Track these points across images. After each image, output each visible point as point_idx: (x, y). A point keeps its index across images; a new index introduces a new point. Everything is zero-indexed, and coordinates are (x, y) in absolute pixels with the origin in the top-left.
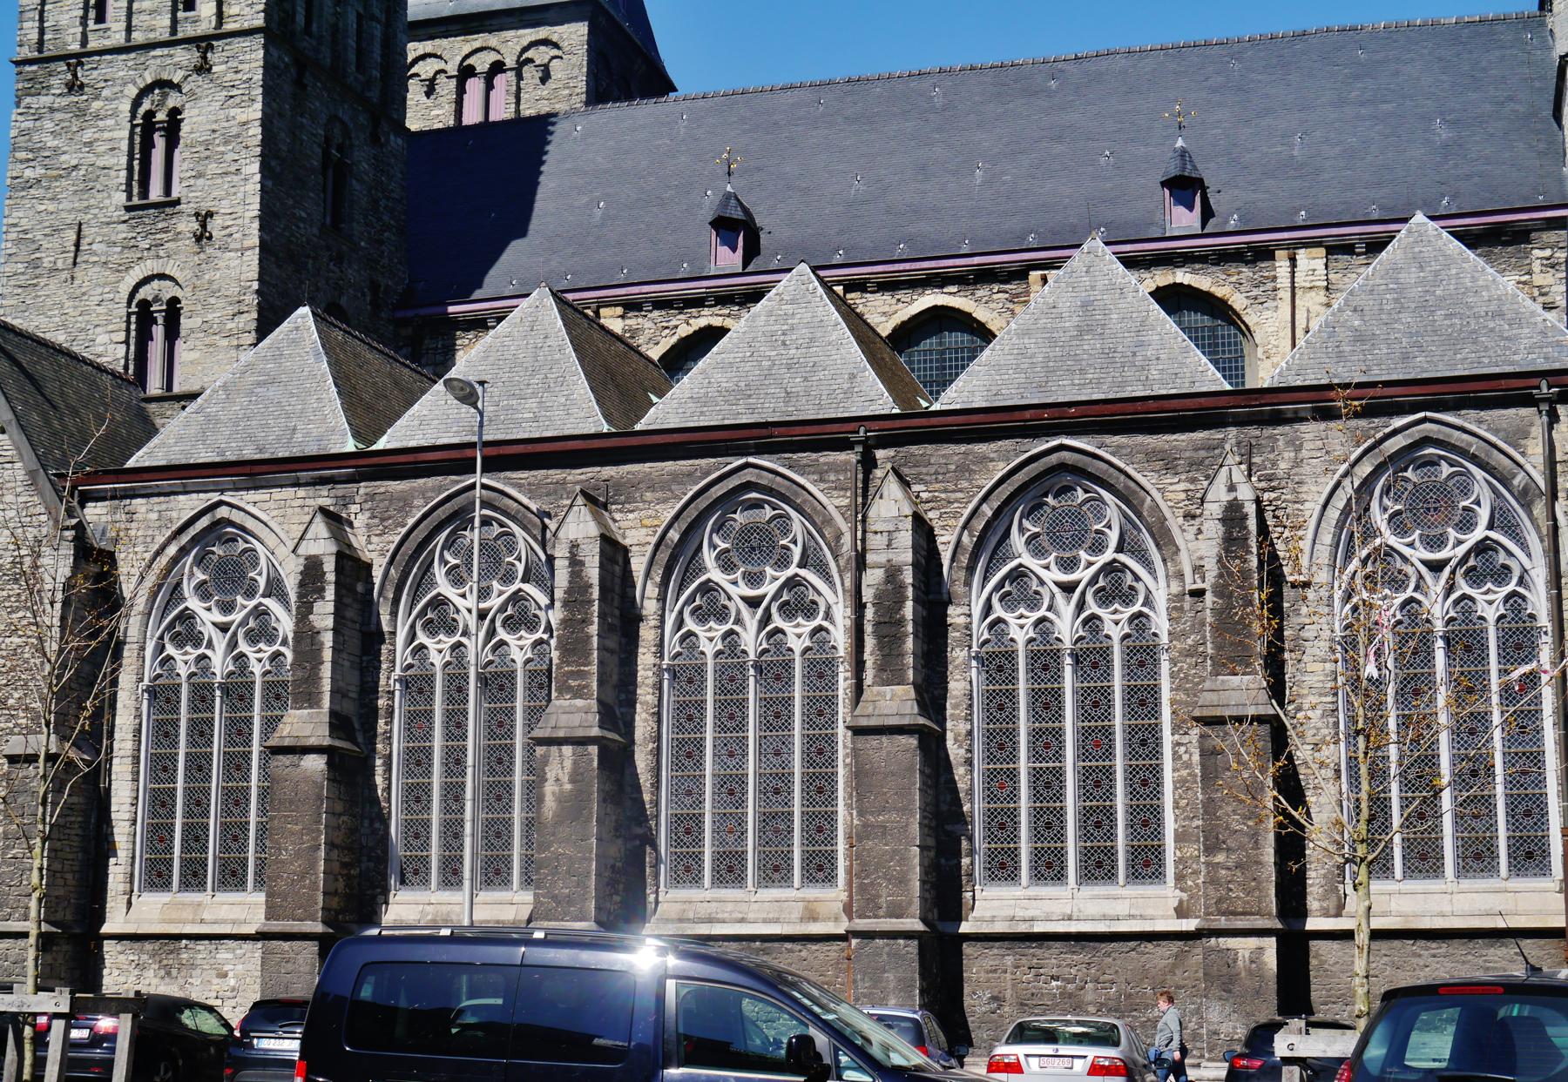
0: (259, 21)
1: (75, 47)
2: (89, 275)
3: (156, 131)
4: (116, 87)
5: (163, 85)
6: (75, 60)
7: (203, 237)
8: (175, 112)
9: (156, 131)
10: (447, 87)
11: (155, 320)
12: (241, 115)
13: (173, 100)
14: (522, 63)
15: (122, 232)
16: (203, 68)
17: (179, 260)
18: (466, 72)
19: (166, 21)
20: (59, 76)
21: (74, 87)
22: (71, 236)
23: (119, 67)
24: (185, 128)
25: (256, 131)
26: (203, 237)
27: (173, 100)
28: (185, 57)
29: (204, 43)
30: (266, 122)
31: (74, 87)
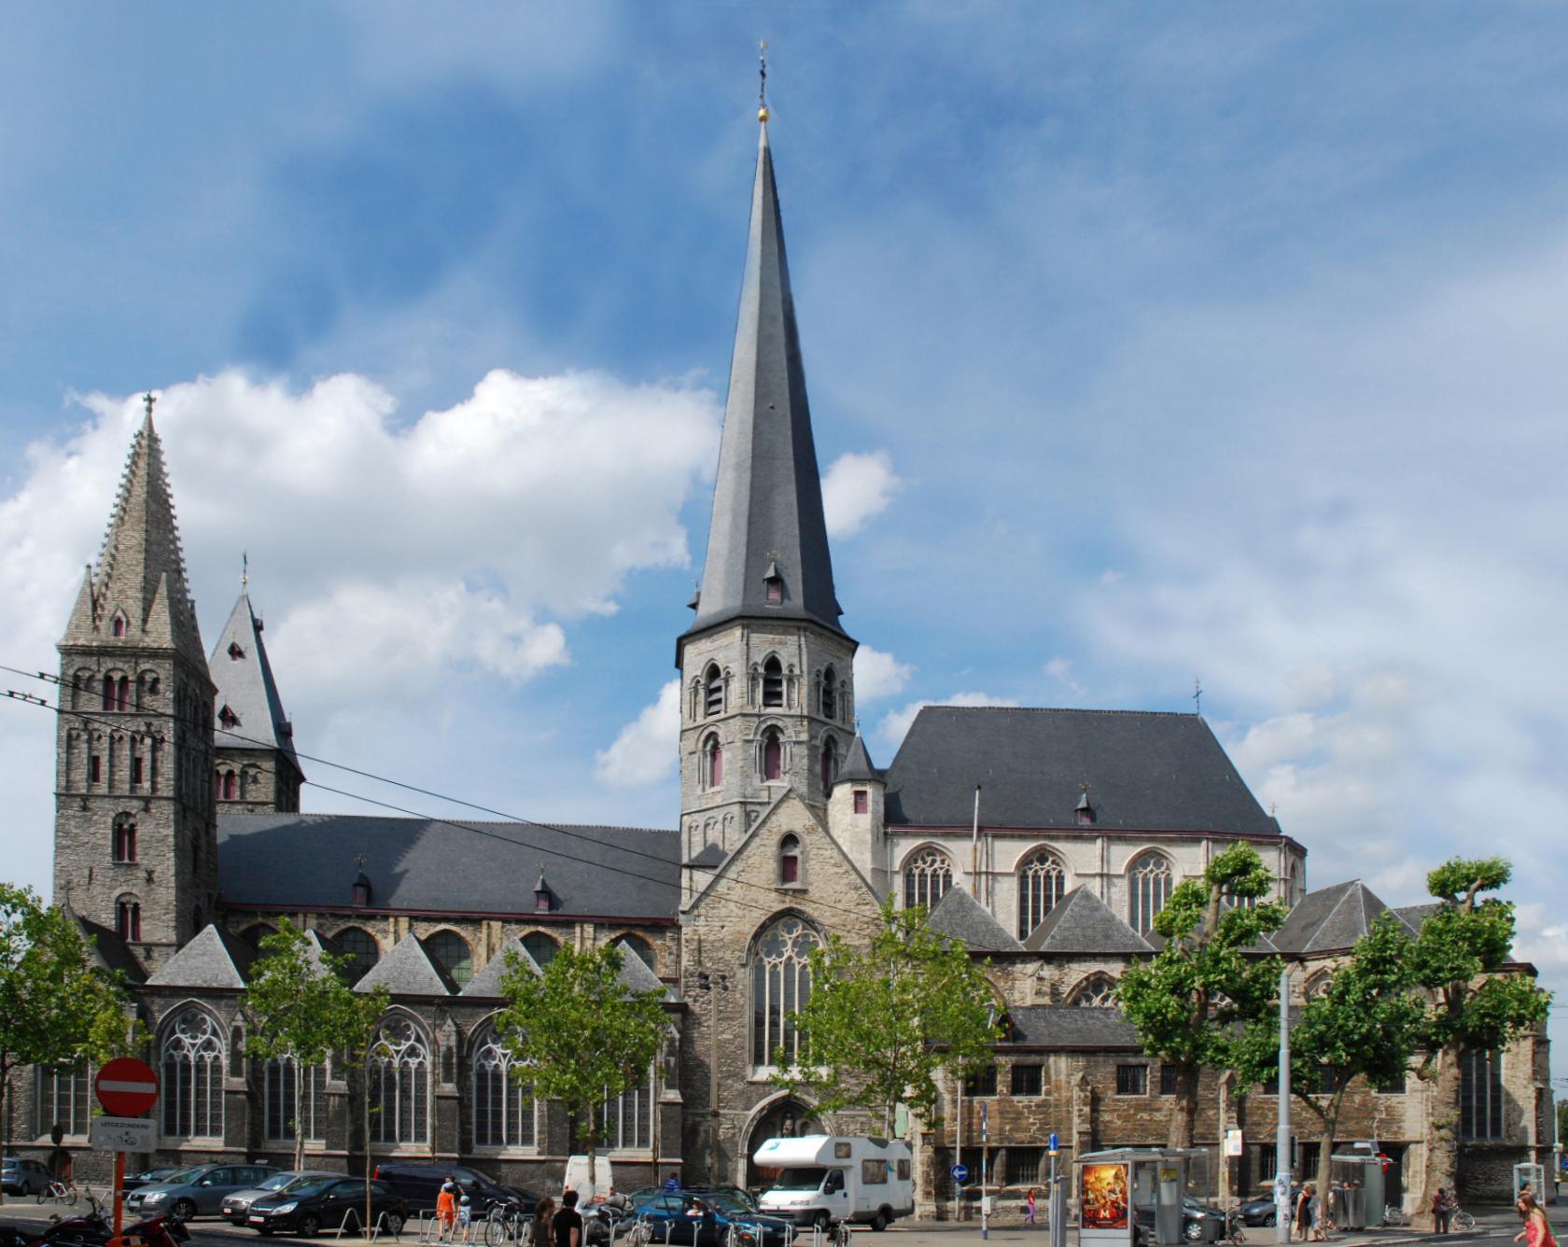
0: (171, 794)
1: (84, 791)
3: (124, 838)
5: (128, 815)
6: (85, 798)
8: (132, 826)
9: (124, 838)
12: (165, 832)
13: (132, 821)
15: (111, 873)
16: (147, 810)
17: (138, 889)
19: (127, 786)
20: (77, 803)
21: (85, 808)
22: (86, 872)
23: (107, 804)
24: (138, 835)
25: (171, 840)
27: (132, 821)
31: (85, 808)
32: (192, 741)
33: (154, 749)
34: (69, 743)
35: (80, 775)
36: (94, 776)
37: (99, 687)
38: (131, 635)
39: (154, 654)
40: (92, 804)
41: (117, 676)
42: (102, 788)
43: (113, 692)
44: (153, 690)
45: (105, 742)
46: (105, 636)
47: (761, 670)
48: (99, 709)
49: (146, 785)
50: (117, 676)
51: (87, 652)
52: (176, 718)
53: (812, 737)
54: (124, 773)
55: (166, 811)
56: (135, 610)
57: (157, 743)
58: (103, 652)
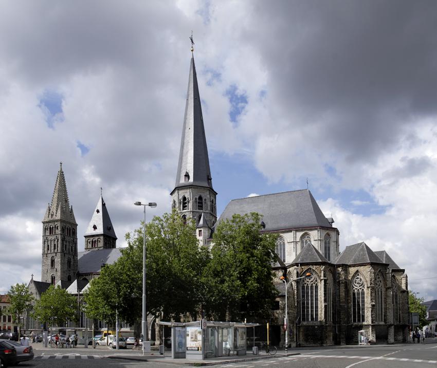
2: (48, 274)
3: (53, 262)
4: (50, 256)
6: (47, 254)
7: (56, 271)
9: (53, 262)
10: (91, 243)
11: (53, 279)
14: (98, 240)
18: (92, 241)
26: (56, 271)
28: (55, 254)
29: (56, 253)
30: (61, 260)
32: (67, 238)
33: (57, 242)
34: (44, 242)
35: (46, 249)
36: (48, 249)
37: (49, 229)
38: (55, 218)
39: (57, 221)
40: (48, 255)
41: (51, 227)
42: (49, 252)
43: (51, 230)
44: (57, 229)
45: (50, 242)
46: (50, 218)
47: (197, 200)
48: (49, 234)
49: (56, 250)
50: (51, 227)
51: (47, 222)
52: (61, 234)
53: (193, 217)
54: (53, 248)
55: (59, 255)
56: (55, 212)
57: (58, 240)
58: (49, 222)
